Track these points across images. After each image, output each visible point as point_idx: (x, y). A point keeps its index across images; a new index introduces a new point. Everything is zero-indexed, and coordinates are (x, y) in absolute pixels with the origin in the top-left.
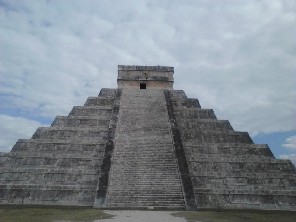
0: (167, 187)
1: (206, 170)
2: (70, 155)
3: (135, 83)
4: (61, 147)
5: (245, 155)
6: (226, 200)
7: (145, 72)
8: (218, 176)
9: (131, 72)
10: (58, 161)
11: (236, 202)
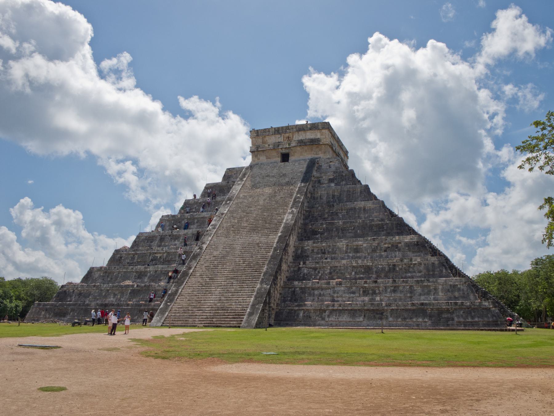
0: (236, 302)
1: (318, 277)
2: (162, 266)
3: (274, 153)
5: (383, 253)
6: (321, 317)
7: (287, 135)
8: (325, 286)
9: (267, 138)
10: (149, 274)
11: (332, 319)
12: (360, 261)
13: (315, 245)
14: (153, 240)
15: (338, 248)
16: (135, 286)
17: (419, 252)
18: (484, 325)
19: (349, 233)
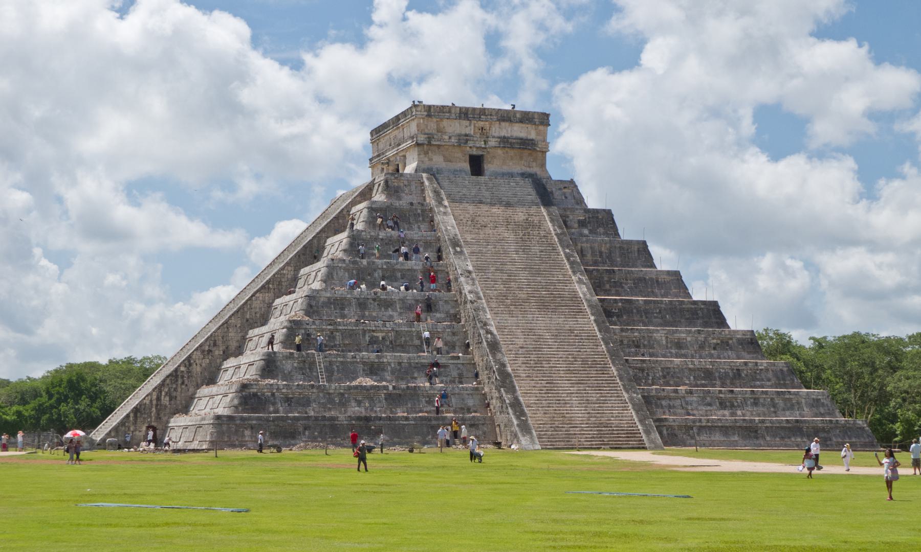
1: (650, 382)
4: (378, 337)
9: (445, 123)
12: (696, 361)
13: (624, 334)
14: (343, 304)
15: (655, 340)
16: (391, 388)
17: (755, 353)
18: (862, 446)
19: (656, 317)
